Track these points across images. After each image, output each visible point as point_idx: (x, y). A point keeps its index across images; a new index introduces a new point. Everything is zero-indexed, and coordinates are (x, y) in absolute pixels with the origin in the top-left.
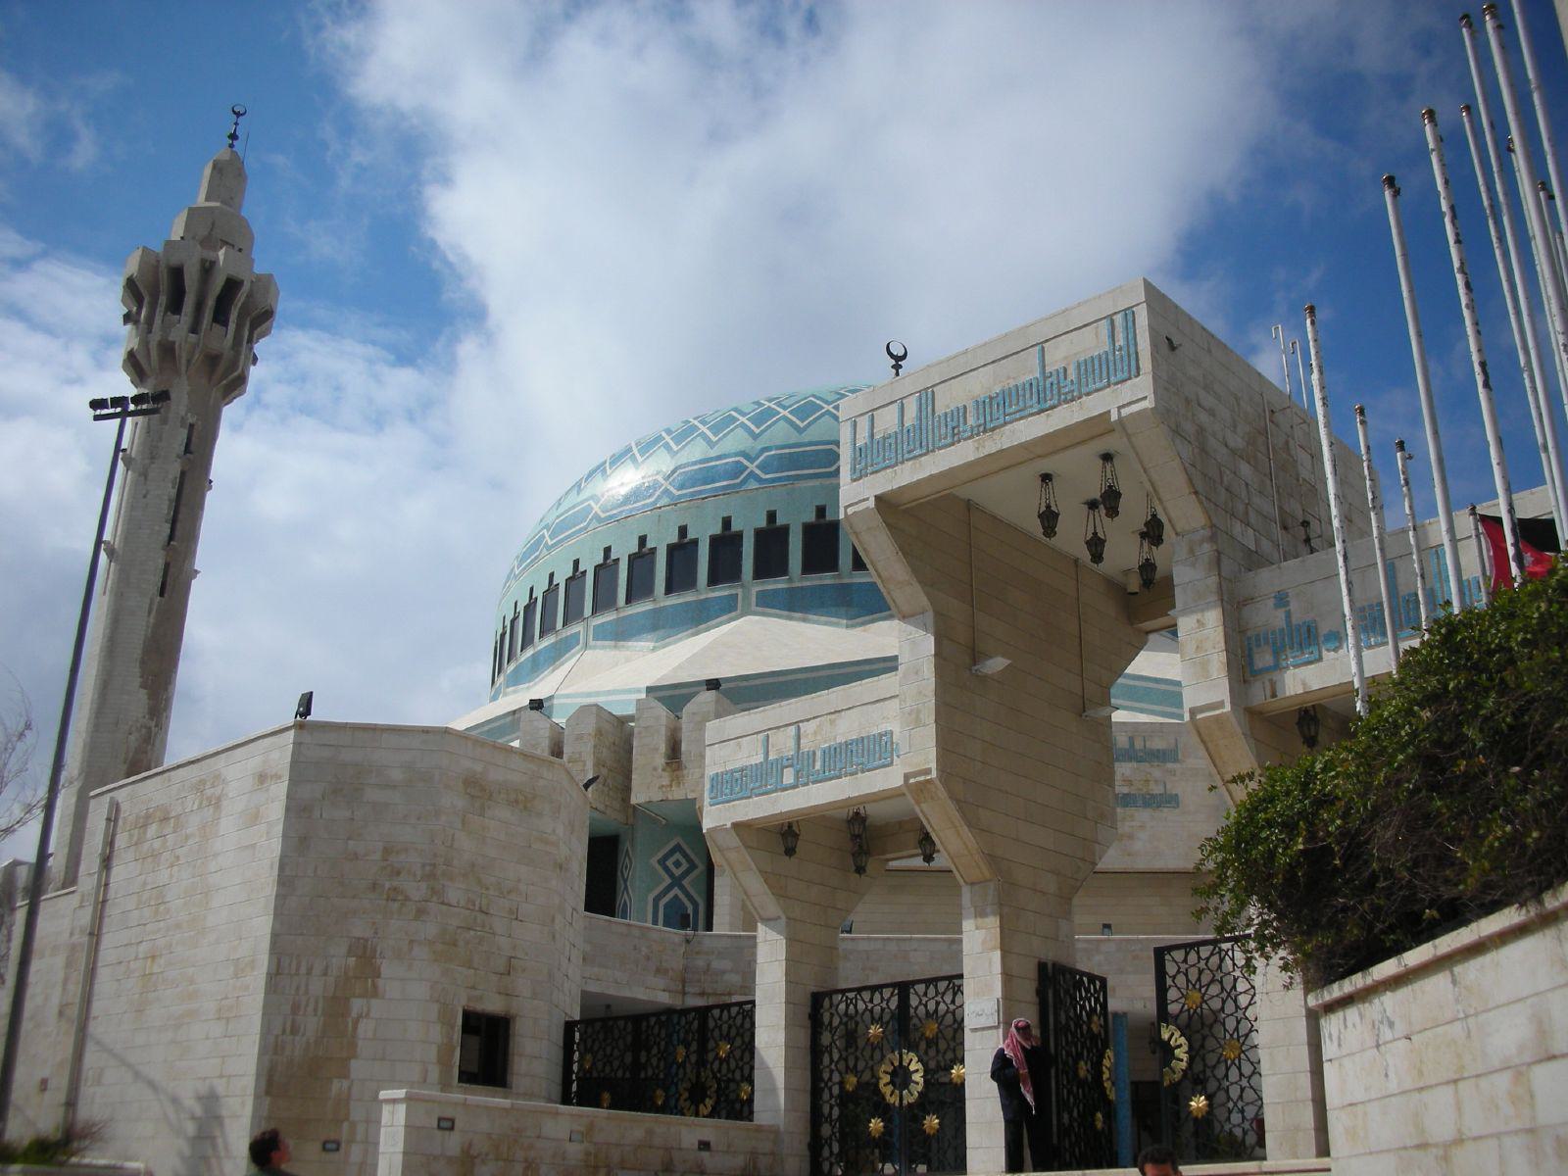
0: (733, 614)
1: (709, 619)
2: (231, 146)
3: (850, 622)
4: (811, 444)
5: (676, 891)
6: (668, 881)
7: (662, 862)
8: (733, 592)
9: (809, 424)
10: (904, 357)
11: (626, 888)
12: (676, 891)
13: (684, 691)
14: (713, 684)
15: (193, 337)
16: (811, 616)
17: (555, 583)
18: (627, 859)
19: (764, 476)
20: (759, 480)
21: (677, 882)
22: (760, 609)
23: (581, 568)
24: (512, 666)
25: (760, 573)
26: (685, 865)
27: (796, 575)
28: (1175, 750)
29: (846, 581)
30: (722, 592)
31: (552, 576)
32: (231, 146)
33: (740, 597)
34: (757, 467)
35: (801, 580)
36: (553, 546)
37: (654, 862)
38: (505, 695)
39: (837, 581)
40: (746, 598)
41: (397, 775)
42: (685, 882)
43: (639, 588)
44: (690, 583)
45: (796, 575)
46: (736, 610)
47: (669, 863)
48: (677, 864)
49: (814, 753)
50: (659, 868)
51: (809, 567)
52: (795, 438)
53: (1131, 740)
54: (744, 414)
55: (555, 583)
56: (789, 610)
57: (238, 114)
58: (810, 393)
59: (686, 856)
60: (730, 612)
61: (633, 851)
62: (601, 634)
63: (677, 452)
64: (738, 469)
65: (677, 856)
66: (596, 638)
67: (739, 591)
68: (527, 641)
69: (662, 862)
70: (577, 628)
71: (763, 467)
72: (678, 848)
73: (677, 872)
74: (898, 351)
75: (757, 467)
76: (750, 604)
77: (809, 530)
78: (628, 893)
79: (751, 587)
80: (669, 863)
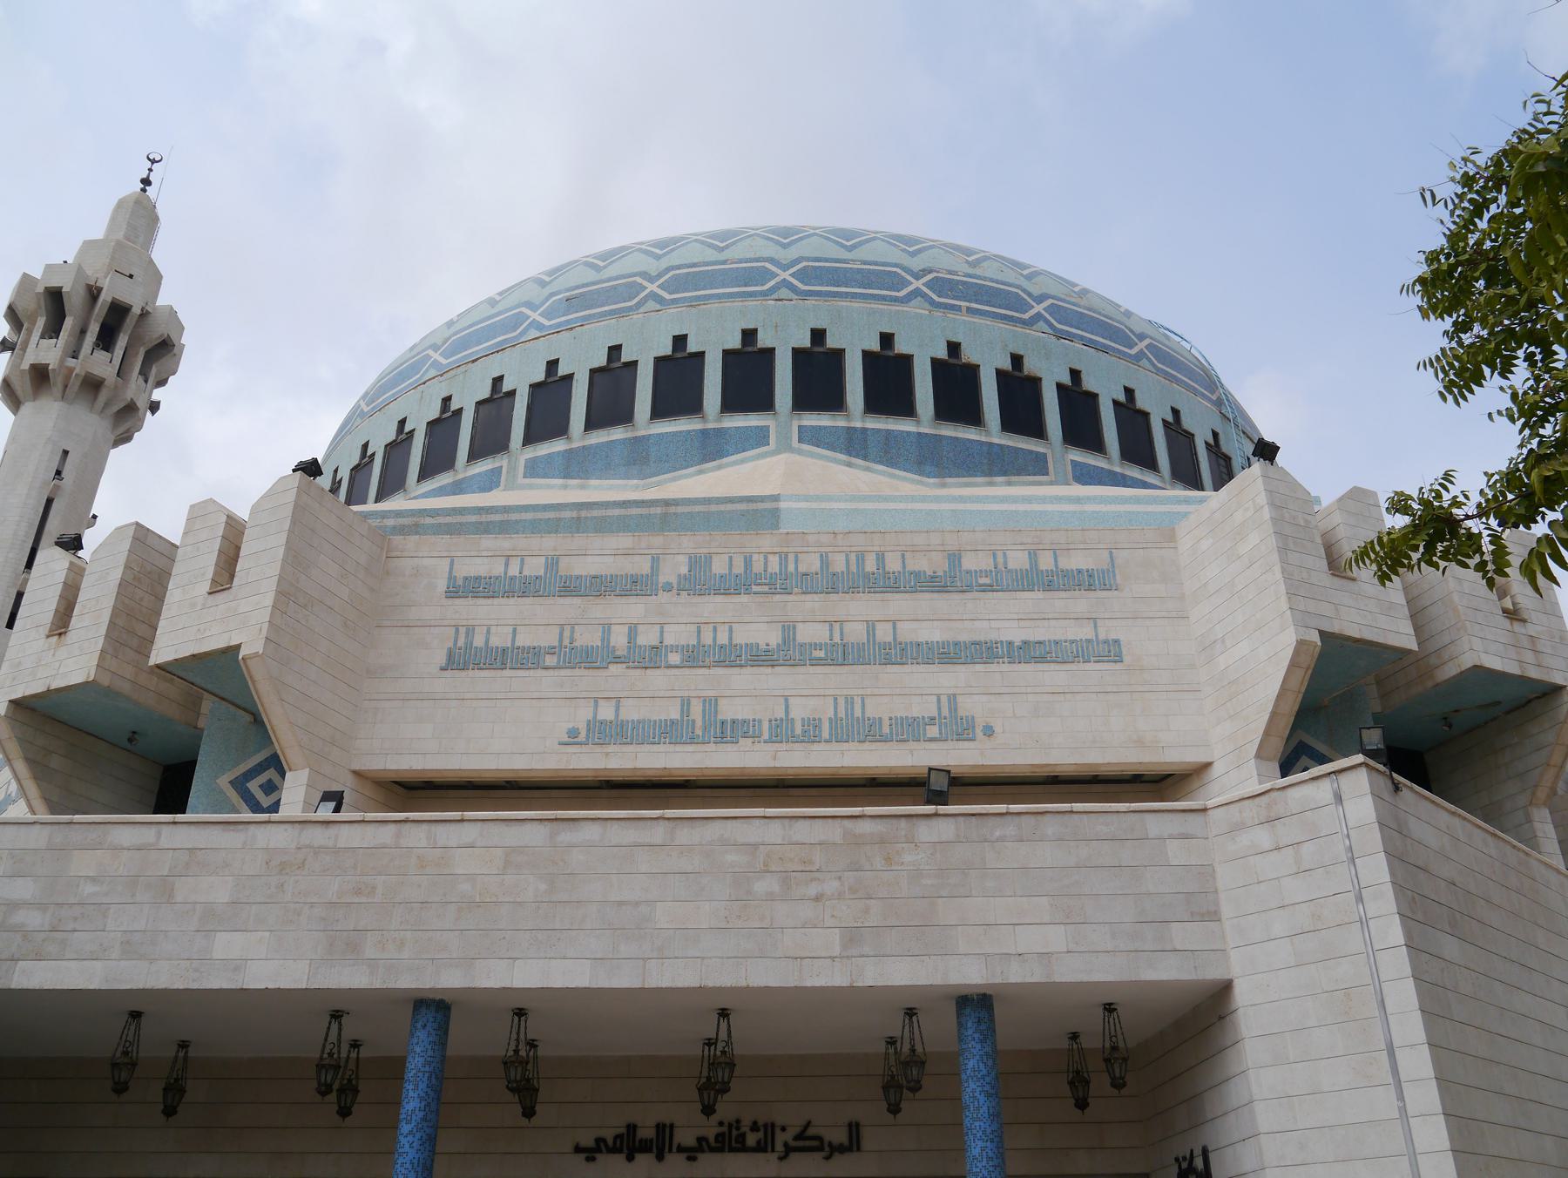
2: (144, 190)
8: (497, 465)
15: (71, 362)
16: (593, 482)
20: (540, 327)
22: (528, 481)
30: (483, 466)
32: (144, 190)
35: (583, 438)
37: (224, 781)
39: (629, 435)
40: (512, 469)
47: (254, 786)
50: (232, 794)
53: (1033, 556)
57: (153, 162)
67: (505, 463)
69: (240, 784)
71: (548, 315)
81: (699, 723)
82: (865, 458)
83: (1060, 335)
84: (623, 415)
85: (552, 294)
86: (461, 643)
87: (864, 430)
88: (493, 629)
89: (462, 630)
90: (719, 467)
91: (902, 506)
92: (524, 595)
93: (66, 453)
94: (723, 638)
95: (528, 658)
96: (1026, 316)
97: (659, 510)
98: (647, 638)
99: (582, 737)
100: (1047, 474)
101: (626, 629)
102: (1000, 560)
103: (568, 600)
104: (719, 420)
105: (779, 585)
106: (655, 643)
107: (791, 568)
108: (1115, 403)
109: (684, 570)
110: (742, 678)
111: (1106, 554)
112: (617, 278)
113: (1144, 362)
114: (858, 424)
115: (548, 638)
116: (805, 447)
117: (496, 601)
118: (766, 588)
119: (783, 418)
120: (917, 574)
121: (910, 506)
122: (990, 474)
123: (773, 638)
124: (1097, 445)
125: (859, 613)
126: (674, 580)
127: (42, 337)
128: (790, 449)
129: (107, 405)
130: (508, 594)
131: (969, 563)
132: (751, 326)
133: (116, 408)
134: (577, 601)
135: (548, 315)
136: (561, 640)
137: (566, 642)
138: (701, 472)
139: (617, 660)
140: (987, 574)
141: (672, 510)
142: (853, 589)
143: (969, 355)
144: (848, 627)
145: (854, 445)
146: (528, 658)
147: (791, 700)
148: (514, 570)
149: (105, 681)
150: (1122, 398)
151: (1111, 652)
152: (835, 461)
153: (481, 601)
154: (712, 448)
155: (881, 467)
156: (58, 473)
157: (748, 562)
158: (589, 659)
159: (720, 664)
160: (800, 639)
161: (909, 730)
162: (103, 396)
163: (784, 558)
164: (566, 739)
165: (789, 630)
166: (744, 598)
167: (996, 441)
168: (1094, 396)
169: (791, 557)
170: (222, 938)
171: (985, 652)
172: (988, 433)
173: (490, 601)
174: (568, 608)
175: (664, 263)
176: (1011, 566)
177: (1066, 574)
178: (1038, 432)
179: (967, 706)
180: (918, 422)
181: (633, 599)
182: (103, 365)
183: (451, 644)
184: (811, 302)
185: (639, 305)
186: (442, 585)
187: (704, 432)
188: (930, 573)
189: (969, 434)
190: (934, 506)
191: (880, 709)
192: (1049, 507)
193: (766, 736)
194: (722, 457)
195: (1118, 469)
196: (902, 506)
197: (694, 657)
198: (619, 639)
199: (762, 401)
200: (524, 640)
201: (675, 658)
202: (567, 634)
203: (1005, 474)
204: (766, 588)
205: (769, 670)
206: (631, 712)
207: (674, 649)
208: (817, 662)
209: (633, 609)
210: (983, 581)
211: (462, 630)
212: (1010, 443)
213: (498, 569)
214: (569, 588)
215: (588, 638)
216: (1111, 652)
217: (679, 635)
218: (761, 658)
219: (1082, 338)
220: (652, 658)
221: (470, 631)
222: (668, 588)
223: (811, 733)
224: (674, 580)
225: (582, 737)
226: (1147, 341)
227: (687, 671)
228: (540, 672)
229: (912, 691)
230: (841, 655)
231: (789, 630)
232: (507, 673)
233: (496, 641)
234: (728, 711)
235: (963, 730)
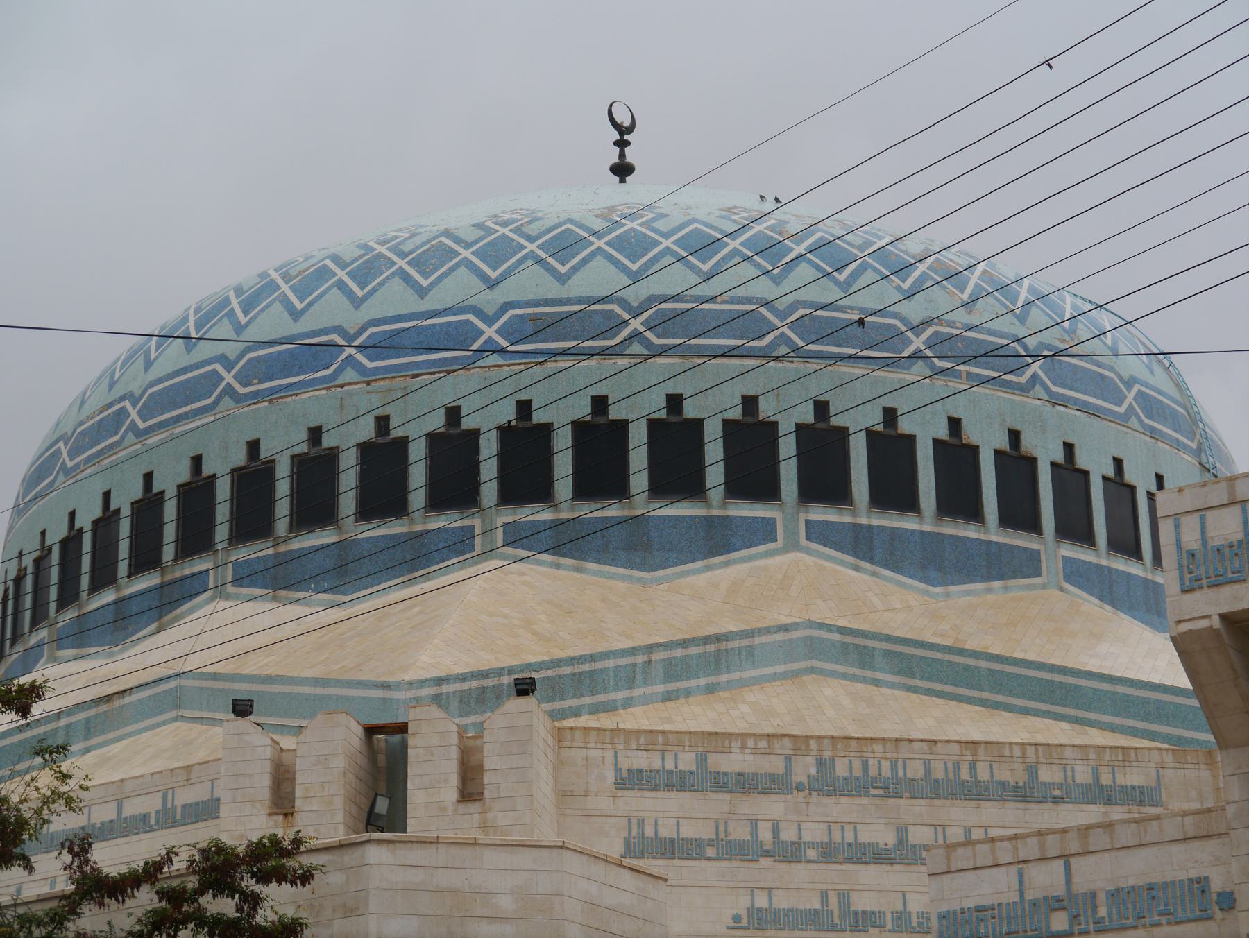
8: (467, 522)
10: (630, 129)
16: (591, 566)
25: (508, 496)
27: (564, 503)
28: (1156, 790)
35: (572, 509)
41: (506, 904)
43: (315, 507)
44: (396, 506)
45: (564, 503)
49: (1094, 895)
51: (583, 491)
52: (553, 290)
54: (467, 246)
58: (564, 217)
62: (245, 576)
67: (477, 522)
70: (201, 564)
74: (623, 119)
79: (494, 517)
81: (836, 913)
82: (872, 561)
86: (634, 832)
87: (870, 527)
88: (660, 821)
89: (634, 821)
90: (727, 564)
91: (938, 656)
92: (682, 789)
94: (849, 838)
95: (690, 849)
96: (1023, 380)
97: (711, 648)
98: (788, 834)
99: (744, 923)
100: (1040, 575)
101: (769, 825)
102: (1069, 774)
103: (720, 796)
104: (723, 506)
105: (894, 788)
106: (795, 839)
107: (901, 773)
108: (1105, 478)
109: (813, 771)
110: (869, 875)
111: (1153, 772)
113: (1133, 422)
114: (863, 520)
115: (704, 832)
116: (814, 546)
117: (660, 794)
118: (881, 792)
119: (787, 512)
120: (1003, 784)
121: (948, 657)
122: (988, 579)
123: (887, 838)
124: (1087, 538)
126: (804, 780)
130: (669, 787)
131: (1046, 775)
132: (752, 393)
134: (727, 796)
136: (717, 834)
137: (722, 835)
138: (709, 568)
139: (767, 854)
140: (1059, 786)
141: (723, 645)
142: (952, 796)
144: (949, 831)
145: (860, 545)
146: (690, 849)
147: (907, 895)
148: (670, 765)
150: (1111, 473)
153: (647, 794)
157: (865, 766)
158: (743, 852)
159: (849, 860)
160: (912, 840)
163: (894, 762)
164: (733, 924)
165: (902, 831)
166: (865, 801)
167: (994, 538)
168: (1086, 474)
169: (900, 763)
173: (653, 794)
174: (719, 803)
176: (1078, 780)
177: (1123, 789)
178: (1032, 525)
180: (921, 520)
181: (774, 797)
183: (625, 834)
186: (610, 776)
187: (708, 520)
188: (1012, 783)
189: (969, 531)
192: (1084, 683)
193: (889, 926)
194: (729, 551)
195: (1104, 562)
196: (938, 656)
197: (829, 853)
198: (765, 835)
199: (768, 491)
200: (687, 832)
201: (811, 854)
202: (722, 828)
203: (1002, 577)
204: (881, 792)
205: (889, 868)
206: (783, 902)
207: (811, 845)
209: (772, 807)
210: (1057, 793)
211: (634, 821)
212: (1007, 541)
213: (657, 764)
214: (720, 783)
215: (740, 832)
217: (813, 832)
218: (881, 857)
219: (1076, 400)
220: (792, 853)
221: (641, 822)
222: (799, 788)
224: (804, 780)
225: (744, 923)
226: (1136, 388)
227: (824, 866)
228: (704, 863)
231: (902, 831)
232: (676, 862)
234: (862, 902)
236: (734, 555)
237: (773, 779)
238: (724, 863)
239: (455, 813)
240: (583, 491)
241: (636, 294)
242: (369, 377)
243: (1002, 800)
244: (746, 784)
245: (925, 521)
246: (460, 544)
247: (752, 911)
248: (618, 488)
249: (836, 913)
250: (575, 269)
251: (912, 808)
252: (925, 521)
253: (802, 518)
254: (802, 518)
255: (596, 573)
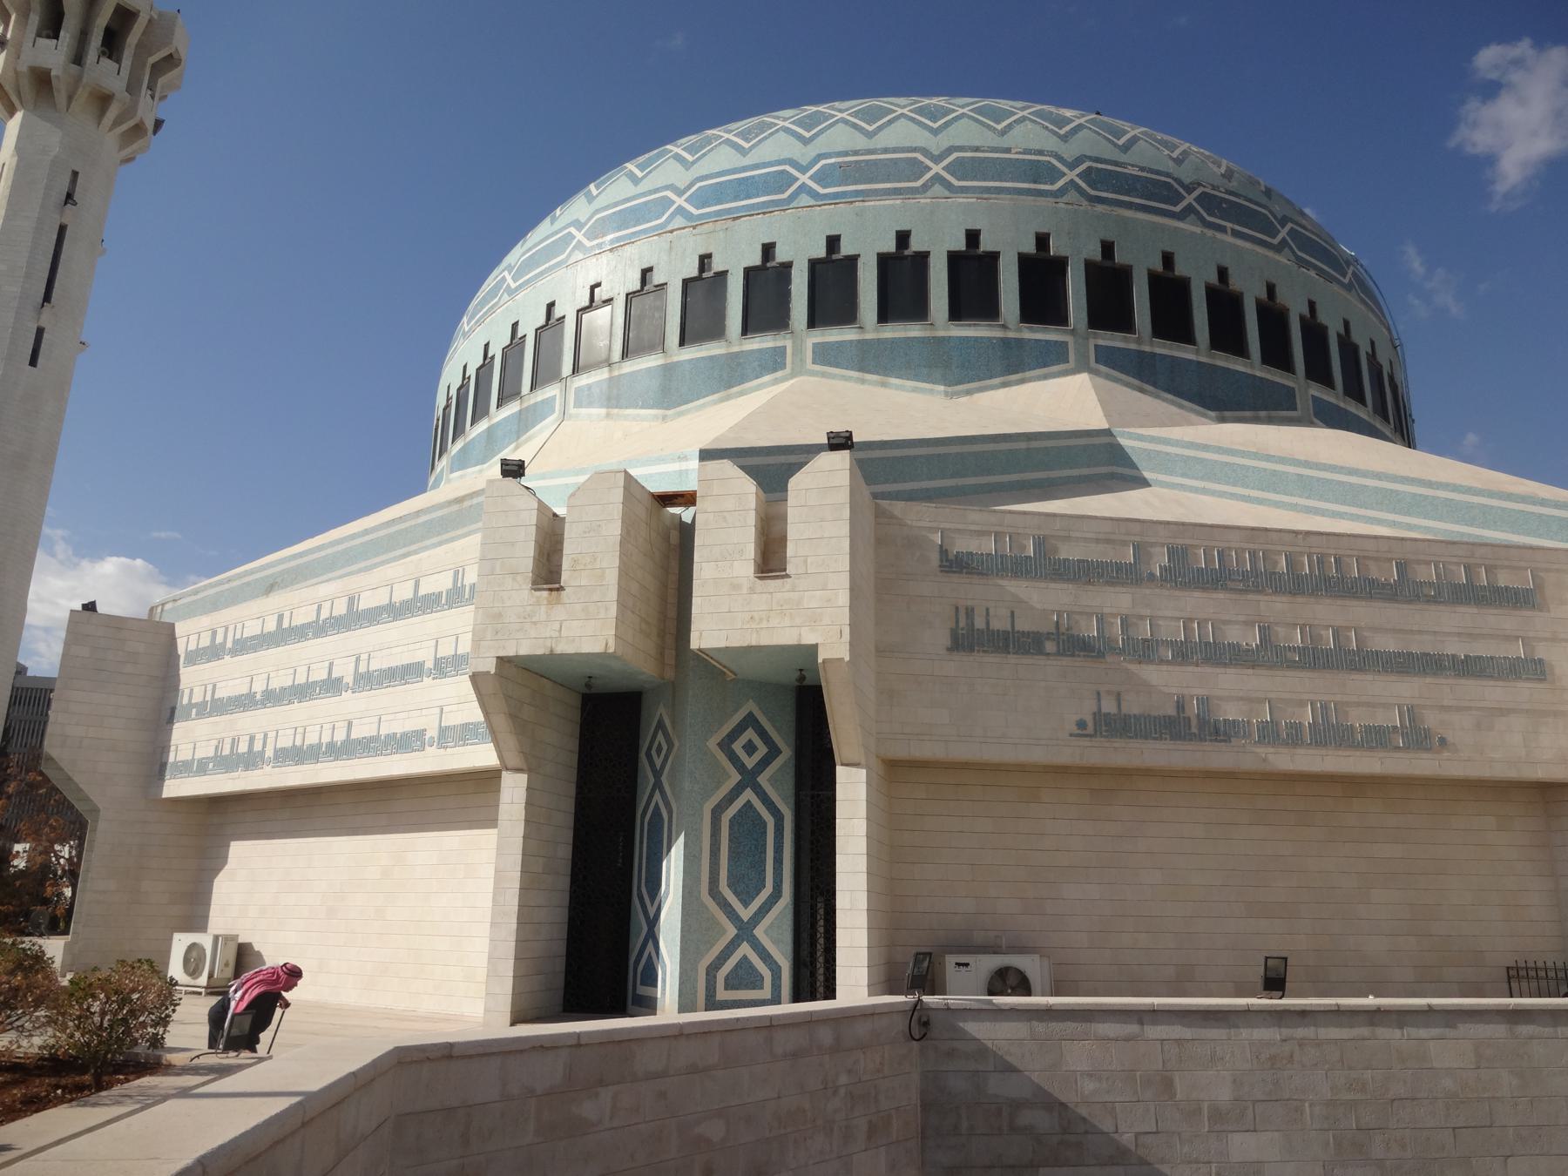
0: (779, 374)
1: (743, 379)
3: (949, 389)
4: (886, 151)
5: (748, 795)
6: (736, 777)
7: (726, 745)
8: (779, 344)
9: (880, 128)
11: (658, 785)
12: (748, 795)
13: (782, 459)
14: (840, 442)
16: (893, 381)
17: (520, 335)
18: (660, 737)
19: (822, 191)
21: (749, 779)
23: (557, 313)
24: (460, 444)
26: (762, 750)
29: (941, 333)
30: (761, 343)
31: (515, 326)
33: (789, 351)
34: (811, 178)
35: (876, 330)
36: (517, 289)
37: (712, 744)
38: (449, 481)
40: (798, 351)
42: (763, 779)
44: (715, 331)
46: (783, 366)
47: (737, 747)
48: (750, 748)
51: (885, 314)
52: (861, 142)
55: (520, 335)
56: (861, 369)
59: (763, 734)
60: (775, 370)
61: (673, 723)
63: (694, 163)
64: (783, 181)
65: (750, 734)
66: (578, 404)
67: (789, 344)
68: (480, 412)
69: (726, 745)
70: (551, 391)
71: (820, 178)
72: (750, 721)
73: (750, 762)
75: (811, 178)
76: (803, 361)
77: (885, 262)
78: (663, 793)
79: (801, 338)
80: (737, 747)
82: (1154, 385)
83: (1301, 263)
84: (917, 309)
85: (820, 157)
86: (962, 624)
87: (1153, 355)
93: (75, 174)
99: (1090, 730)
100: (1295, 409)
112: (895, 150)
114: (1147, 349)
116: (1103, 368)
118: (1241, 586)
125: (1327, 614)
127: (39, 35)
128: (1091, 371)
129: (117, 122)
133: (125, 127)
135: (820, 178)
138: (1005, 385)
143: (1235, 283)
149: (619, 653)
151: (1535, 669)
152: (1127, 385)
154: (1014, 362)
155: (1170, 397)
156: (69, 197)
161: (1377, 738)
162: (113, 112)
163: (1253, 554)
167: (1258, 374)
170: (1236, 1139)
171: (1431, 665)
172: (1252, 366)
175: (944, 141)
179: (1431, 720)
182: (106, 74)
184: (1100, 208)
185: (925, 187)
187: (1005, 342)
190: (1279, 467)
191: (1358, 719)
194: (1023, 371)
197: (1184, 654)
205: (1250, 671)
208: (1292, 665)
209: (1118, 601)
212: (1269, 377)
216: (1535, 669)
221: (970, 612)
223: (1294, 737)
228: (1040, 660)
229: (1381, 698)
230: (1314, 659)
231: (1265, 632)
233: (996, 625)
235: (1419, 738)
236: (1028, 374)
237: (1119, 567)
238: (1066, 661)
239: (752, 590)
240: (885, 314)
241: (936, 144)
242: (695, 223)
243: (1371, 597)
244: (1085, 573)
245: (1198, 353)
246: (774, 362)
247: (1098, 716)
248: (917, 309)
249: (1194, 722)
250: (880, 128)
251: (1275, 607)
252: (1198, 353)
253: (1092, 343)
254: (1092, 343)
255: (898, 388)
